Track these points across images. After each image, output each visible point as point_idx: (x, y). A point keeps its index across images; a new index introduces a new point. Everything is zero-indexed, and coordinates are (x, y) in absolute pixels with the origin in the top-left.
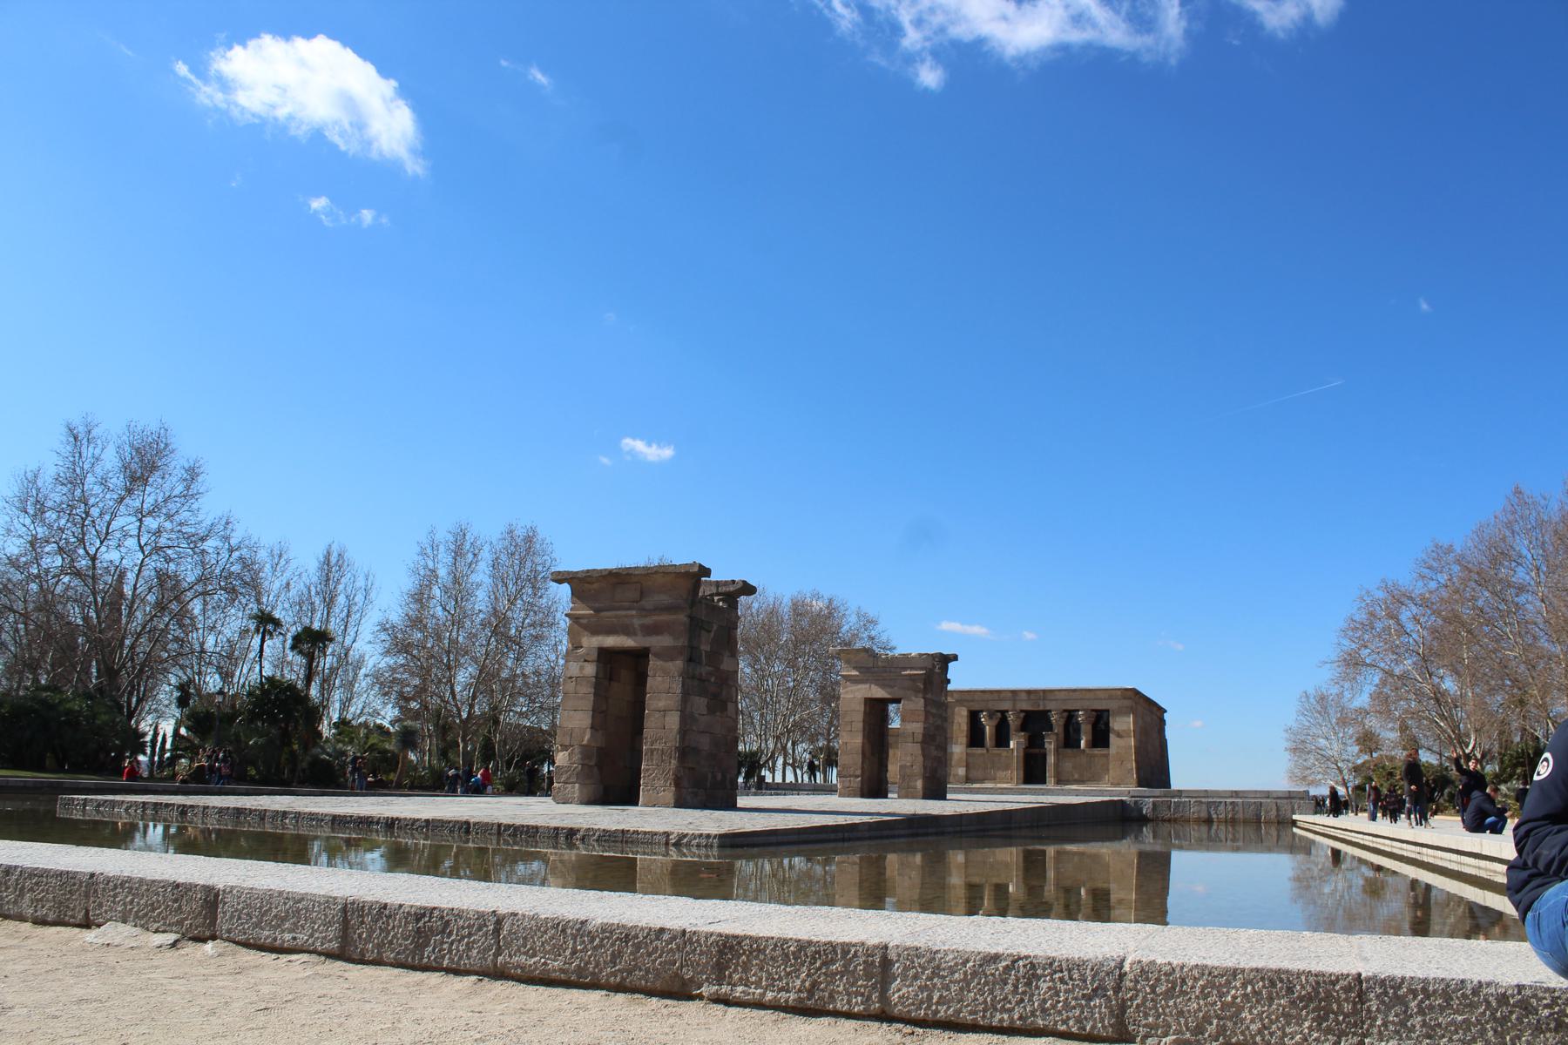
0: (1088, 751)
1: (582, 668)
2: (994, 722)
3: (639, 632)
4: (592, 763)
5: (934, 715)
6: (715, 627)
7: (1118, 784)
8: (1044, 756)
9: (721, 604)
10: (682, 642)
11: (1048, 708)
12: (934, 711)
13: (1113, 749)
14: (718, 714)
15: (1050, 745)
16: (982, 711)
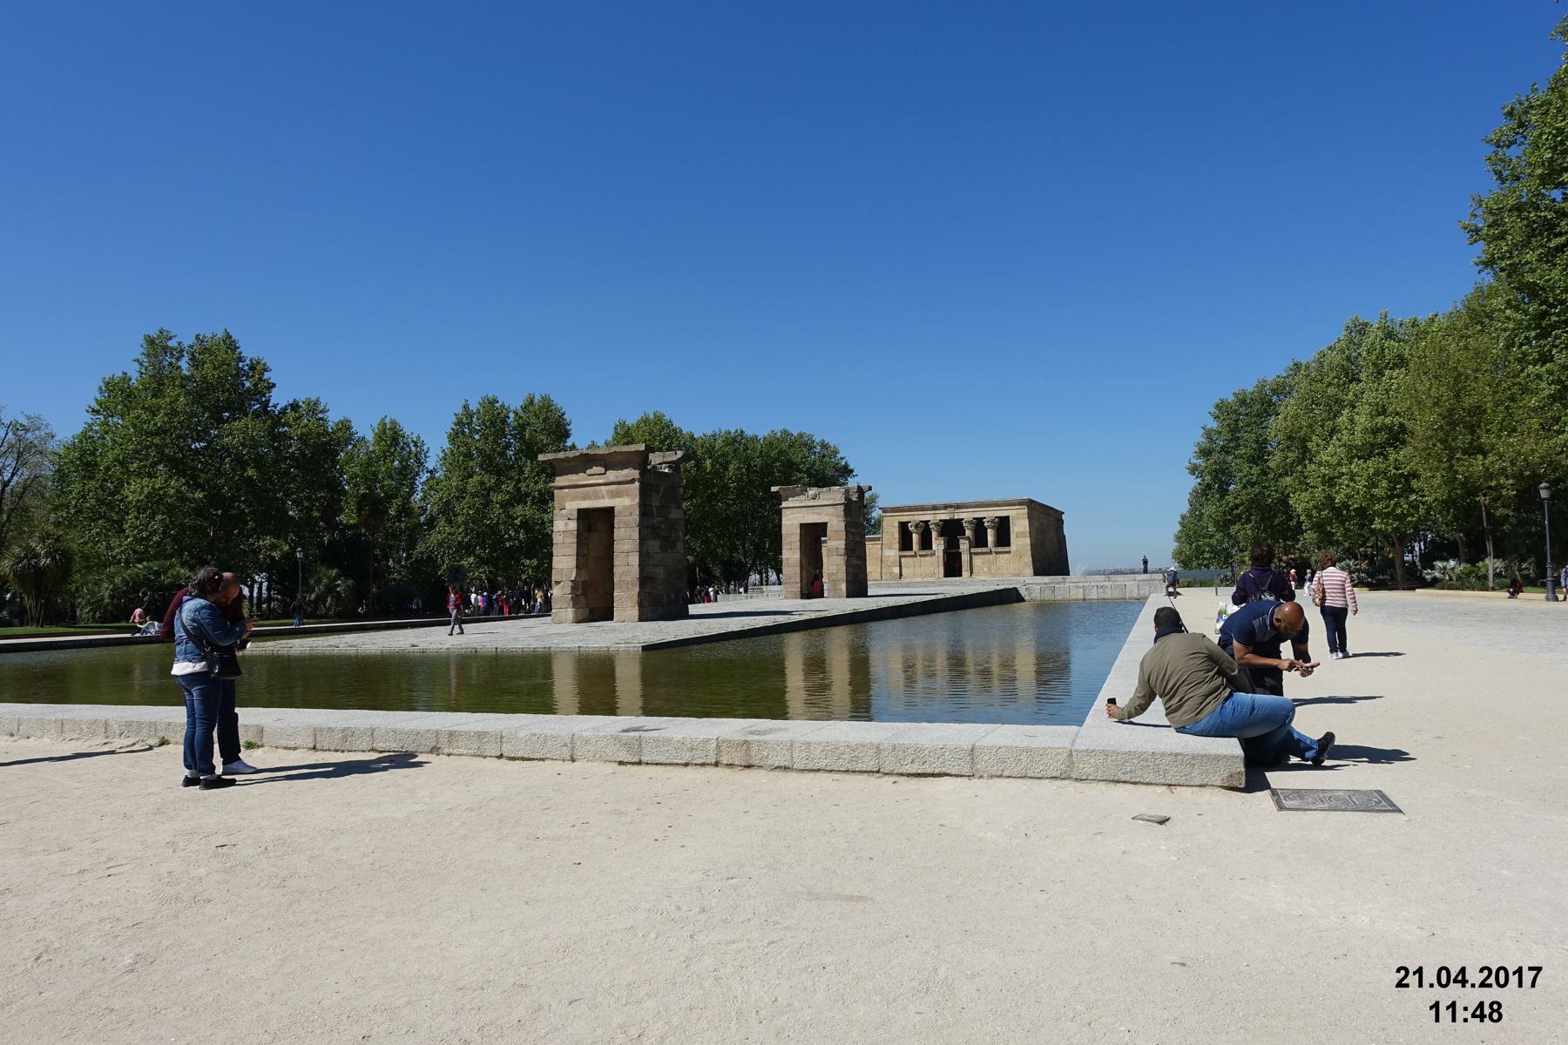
0: (994, 550)
1: (566, 525)
2: (921, 530)
3: (606, 496)
4: (580, 593)
5: (853, 534)
6: (662, 488)
7: (1019, 575)
8: (960, 554)
9: (667, 471)
10: (637, 500)
11: (961, 517)
12: (853, 530)
13: (1013, 548)
14: (669, 551)
15: (964, 546)
16: (910, 522)
